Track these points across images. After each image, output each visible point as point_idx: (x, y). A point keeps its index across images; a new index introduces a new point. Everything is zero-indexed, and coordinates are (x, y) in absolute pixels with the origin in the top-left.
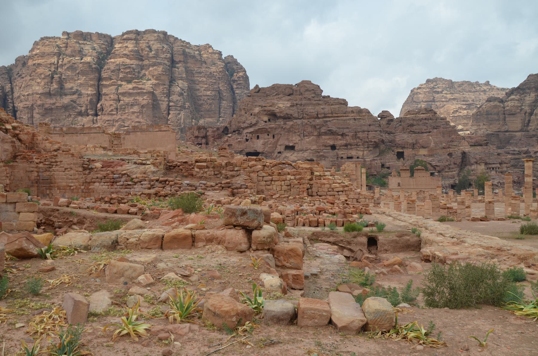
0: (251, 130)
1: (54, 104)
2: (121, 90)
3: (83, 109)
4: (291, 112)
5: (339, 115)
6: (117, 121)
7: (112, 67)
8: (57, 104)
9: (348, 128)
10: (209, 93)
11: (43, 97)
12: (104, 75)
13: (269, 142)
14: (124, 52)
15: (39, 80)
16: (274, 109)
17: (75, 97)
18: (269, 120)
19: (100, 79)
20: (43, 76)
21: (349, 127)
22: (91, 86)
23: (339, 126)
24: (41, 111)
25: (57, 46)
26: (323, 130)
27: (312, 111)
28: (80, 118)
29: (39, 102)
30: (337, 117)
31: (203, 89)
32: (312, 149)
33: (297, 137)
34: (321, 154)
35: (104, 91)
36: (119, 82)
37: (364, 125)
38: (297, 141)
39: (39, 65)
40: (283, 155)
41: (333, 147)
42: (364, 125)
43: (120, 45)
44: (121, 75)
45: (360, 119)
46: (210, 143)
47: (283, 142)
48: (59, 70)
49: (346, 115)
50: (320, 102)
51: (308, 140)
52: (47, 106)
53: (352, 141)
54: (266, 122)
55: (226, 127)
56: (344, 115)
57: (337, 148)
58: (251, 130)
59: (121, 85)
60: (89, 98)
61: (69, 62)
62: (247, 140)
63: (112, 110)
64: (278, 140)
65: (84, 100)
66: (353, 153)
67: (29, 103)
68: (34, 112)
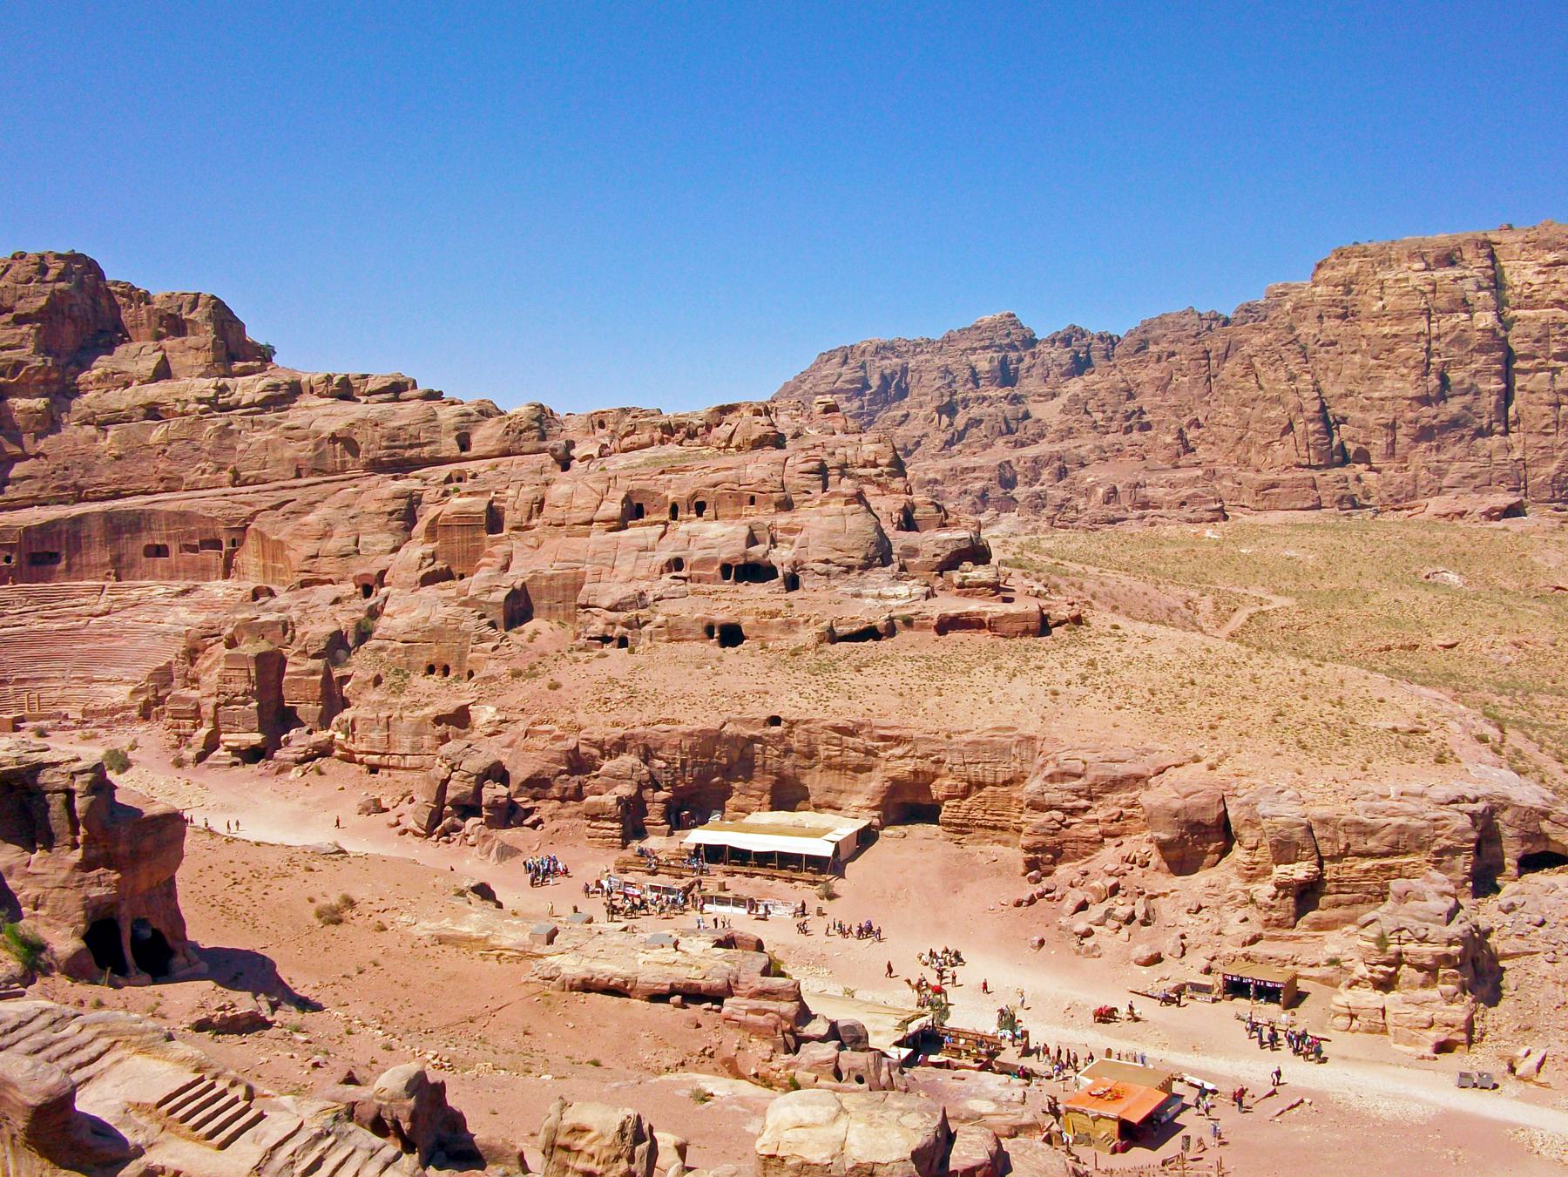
1: (1435, 417)
2: (1559, 386)
3: (1485, 421)
6: (1560, 448)
7: (1536, 334)
8: (1442, 417)
11: (1415, 404)
12: (1519, 347)
14: (1555, 295)
15: (1405, 371)
17: (1468, 398)
19: (1509, 357)
20: (1411, 362)
22: (1497, 373)
24: (1412, 431)
25: (1423, 293)
28: (1479, 441)
29: (1410, 415)
35: (1519, 381)
36: (1552, 363)
39: (1395, 336)
43: (1542, 278)
44: (1555, 349)
48: (1434, 345)
52: (1424, 421)
59: (1555, 370)
60: (1494, 398)
61: (1454, 327)
63: (1547, 426)
65: (1488, 403)
67: (1388, 417)
68: (1399, 432)
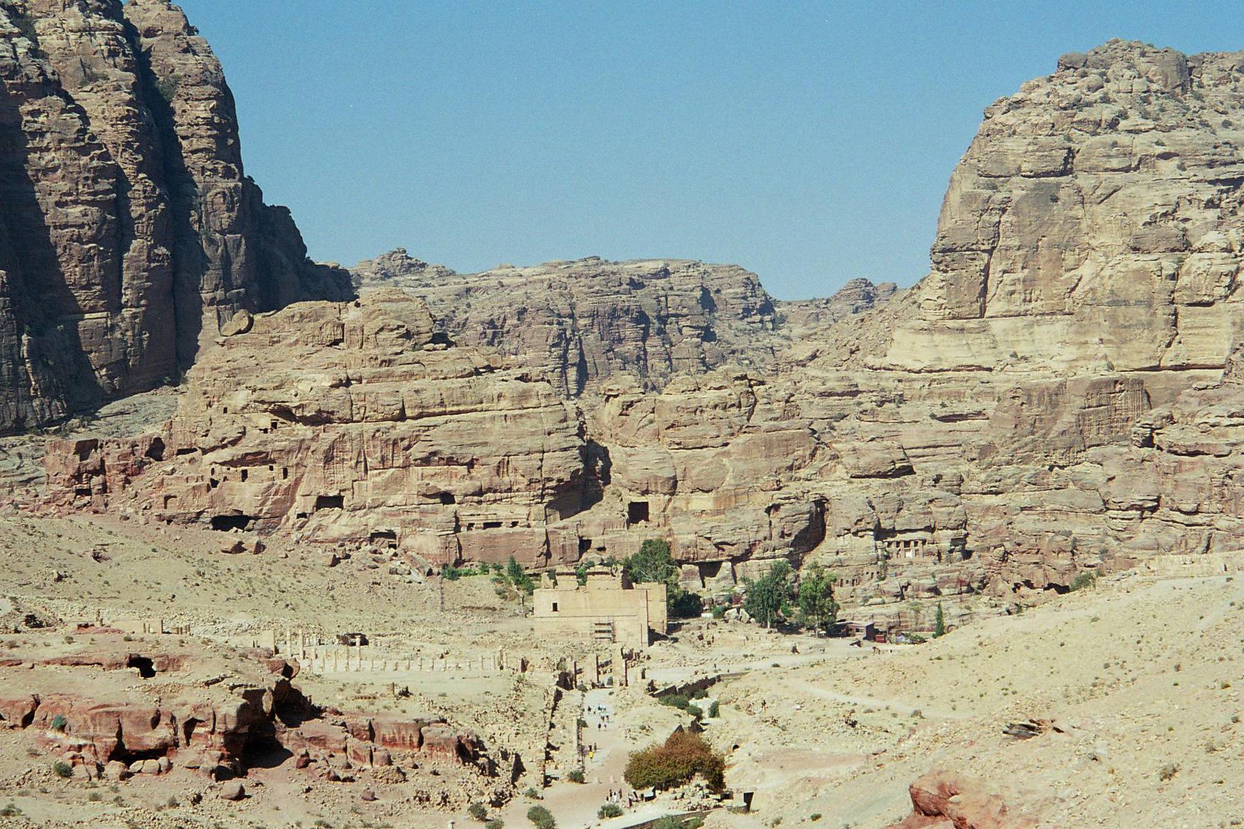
0: (226, 454)
4: (330, 404)
5: (462, 408)
9: (485, 444)
10: (76, 211)
13: (273, 490)
16: (286, 398)
18: (274, 425)
21: (490, 439)
23: (466, 441)
26: (418, 451)
27: (391, 400)
30: (459, 412)
31: (54, 198)
32: (390, 502)
33: (348, 472)
34: (416, 516)
37: (533, 434)
38: (348, 484)
40: (313, 522)
41: (447, 498)
42: (533, 434)
45: (521, 416)
46: (116, 488)
47: (313, 485)
49: (484, 406)
50: (416, 368)
51: (378, 479)
53: (496, 479)
54: (265, 431)
55: (158, 440)
56: (479, 407)
57: (457, 499)
58: (226, 454)
62: (214, 483)
64: (297, 482)
66: (501, 511)
